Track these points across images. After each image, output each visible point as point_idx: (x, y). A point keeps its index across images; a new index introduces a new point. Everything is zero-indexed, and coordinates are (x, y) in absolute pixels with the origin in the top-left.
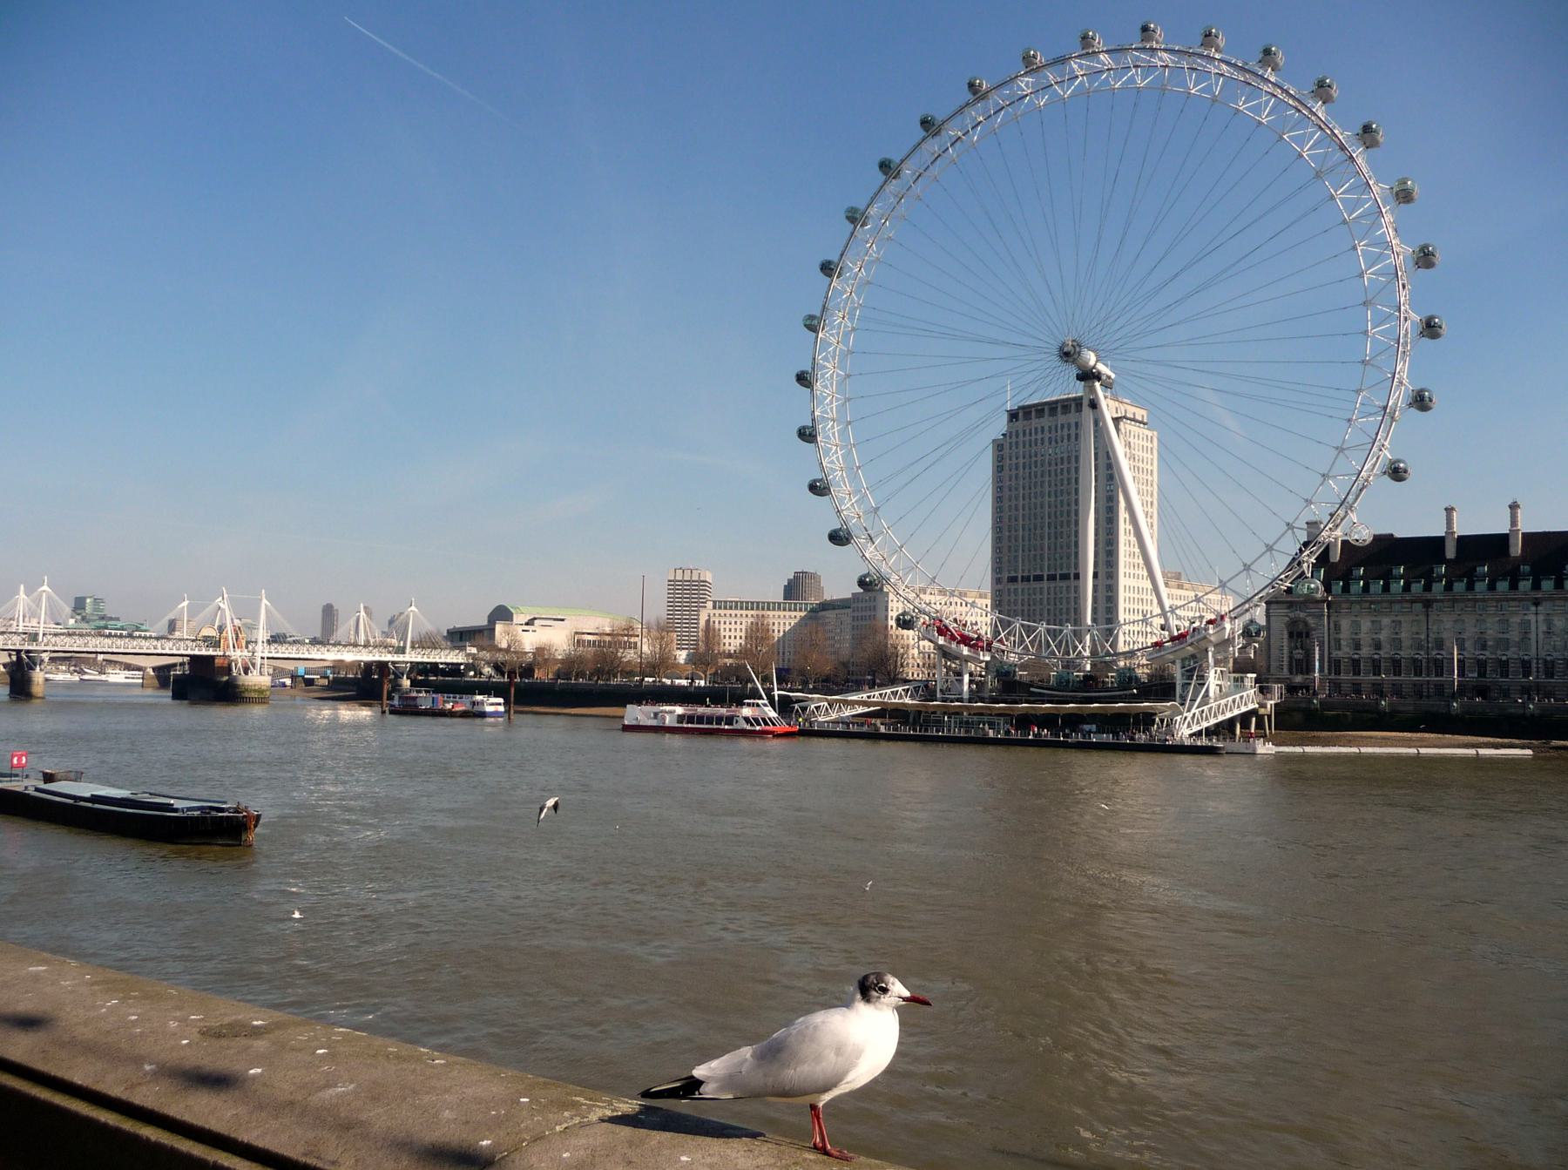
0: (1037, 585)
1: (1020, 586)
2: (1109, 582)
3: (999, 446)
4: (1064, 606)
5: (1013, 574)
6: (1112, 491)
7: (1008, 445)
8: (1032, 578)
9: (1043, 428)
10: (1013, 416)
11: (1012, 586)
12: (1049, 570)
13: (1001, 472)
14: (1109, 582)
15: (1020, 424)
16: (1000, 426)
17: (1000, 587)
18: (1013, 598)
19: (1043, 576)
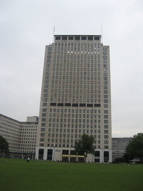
0: (68, 108)
1: (57, 107)
2: (106, 109)
3: (49, 48)
4: (82, 119)
5: (53, 102)
6: (106, 71)
7: (54, 48)
8: (64, 105)
9: (72, 44)
10: (57, 37)
11: (53, 107)
12: (73, 102)
13: (49, 58)
14: (106, 109)
15: (61, 41)
16: (51, 41)
17: (45, 107)
18: (53, 112)
19: (71, 104)
